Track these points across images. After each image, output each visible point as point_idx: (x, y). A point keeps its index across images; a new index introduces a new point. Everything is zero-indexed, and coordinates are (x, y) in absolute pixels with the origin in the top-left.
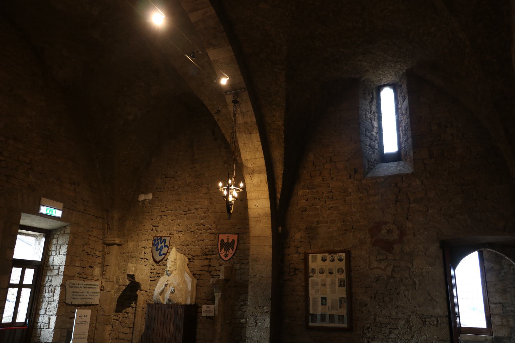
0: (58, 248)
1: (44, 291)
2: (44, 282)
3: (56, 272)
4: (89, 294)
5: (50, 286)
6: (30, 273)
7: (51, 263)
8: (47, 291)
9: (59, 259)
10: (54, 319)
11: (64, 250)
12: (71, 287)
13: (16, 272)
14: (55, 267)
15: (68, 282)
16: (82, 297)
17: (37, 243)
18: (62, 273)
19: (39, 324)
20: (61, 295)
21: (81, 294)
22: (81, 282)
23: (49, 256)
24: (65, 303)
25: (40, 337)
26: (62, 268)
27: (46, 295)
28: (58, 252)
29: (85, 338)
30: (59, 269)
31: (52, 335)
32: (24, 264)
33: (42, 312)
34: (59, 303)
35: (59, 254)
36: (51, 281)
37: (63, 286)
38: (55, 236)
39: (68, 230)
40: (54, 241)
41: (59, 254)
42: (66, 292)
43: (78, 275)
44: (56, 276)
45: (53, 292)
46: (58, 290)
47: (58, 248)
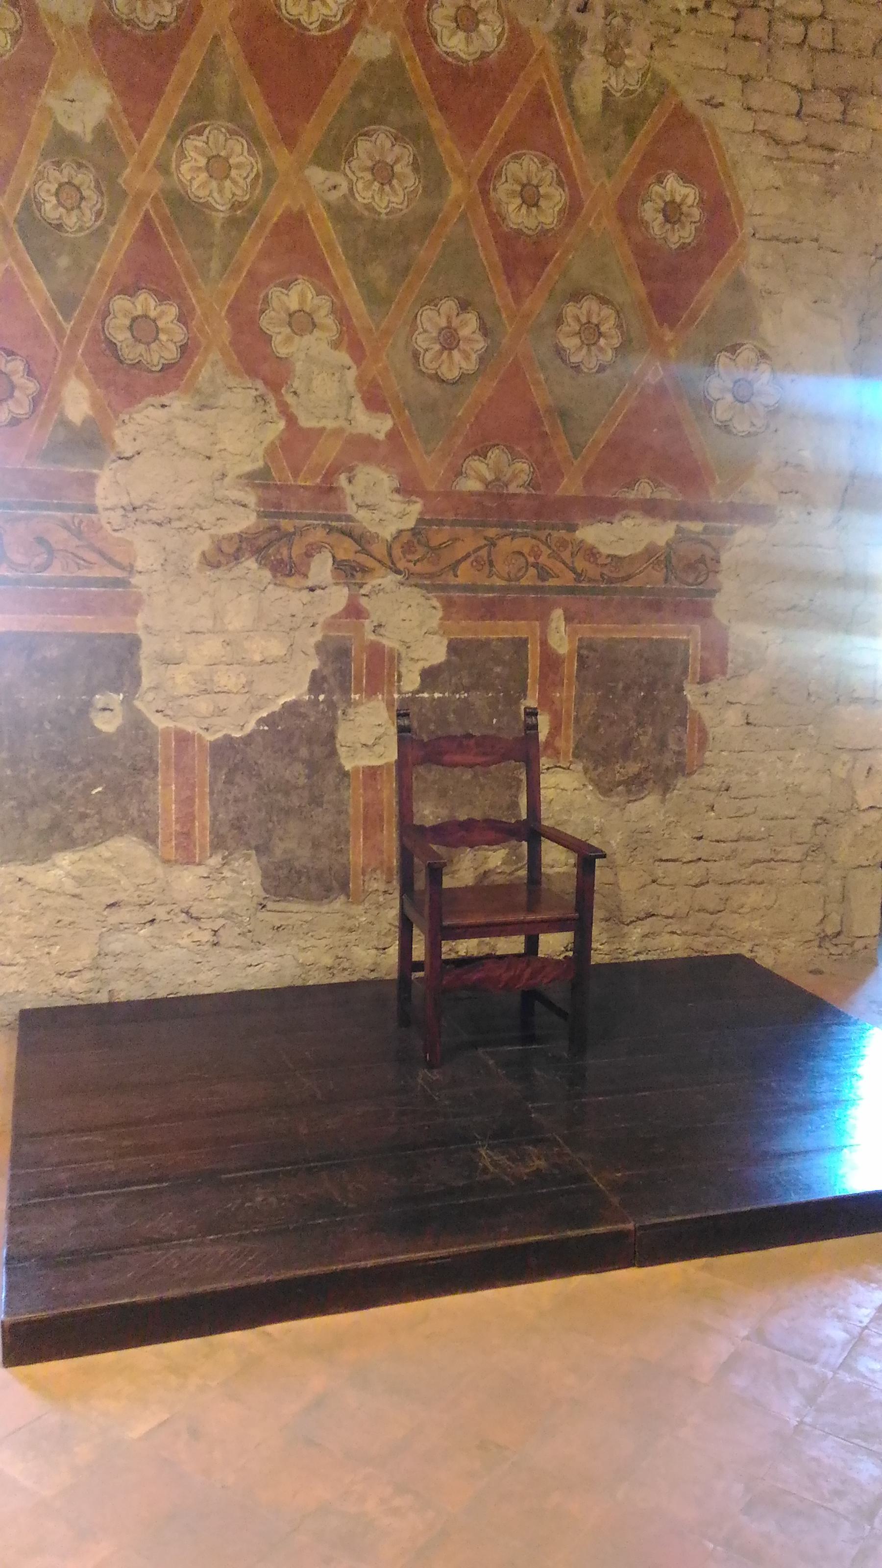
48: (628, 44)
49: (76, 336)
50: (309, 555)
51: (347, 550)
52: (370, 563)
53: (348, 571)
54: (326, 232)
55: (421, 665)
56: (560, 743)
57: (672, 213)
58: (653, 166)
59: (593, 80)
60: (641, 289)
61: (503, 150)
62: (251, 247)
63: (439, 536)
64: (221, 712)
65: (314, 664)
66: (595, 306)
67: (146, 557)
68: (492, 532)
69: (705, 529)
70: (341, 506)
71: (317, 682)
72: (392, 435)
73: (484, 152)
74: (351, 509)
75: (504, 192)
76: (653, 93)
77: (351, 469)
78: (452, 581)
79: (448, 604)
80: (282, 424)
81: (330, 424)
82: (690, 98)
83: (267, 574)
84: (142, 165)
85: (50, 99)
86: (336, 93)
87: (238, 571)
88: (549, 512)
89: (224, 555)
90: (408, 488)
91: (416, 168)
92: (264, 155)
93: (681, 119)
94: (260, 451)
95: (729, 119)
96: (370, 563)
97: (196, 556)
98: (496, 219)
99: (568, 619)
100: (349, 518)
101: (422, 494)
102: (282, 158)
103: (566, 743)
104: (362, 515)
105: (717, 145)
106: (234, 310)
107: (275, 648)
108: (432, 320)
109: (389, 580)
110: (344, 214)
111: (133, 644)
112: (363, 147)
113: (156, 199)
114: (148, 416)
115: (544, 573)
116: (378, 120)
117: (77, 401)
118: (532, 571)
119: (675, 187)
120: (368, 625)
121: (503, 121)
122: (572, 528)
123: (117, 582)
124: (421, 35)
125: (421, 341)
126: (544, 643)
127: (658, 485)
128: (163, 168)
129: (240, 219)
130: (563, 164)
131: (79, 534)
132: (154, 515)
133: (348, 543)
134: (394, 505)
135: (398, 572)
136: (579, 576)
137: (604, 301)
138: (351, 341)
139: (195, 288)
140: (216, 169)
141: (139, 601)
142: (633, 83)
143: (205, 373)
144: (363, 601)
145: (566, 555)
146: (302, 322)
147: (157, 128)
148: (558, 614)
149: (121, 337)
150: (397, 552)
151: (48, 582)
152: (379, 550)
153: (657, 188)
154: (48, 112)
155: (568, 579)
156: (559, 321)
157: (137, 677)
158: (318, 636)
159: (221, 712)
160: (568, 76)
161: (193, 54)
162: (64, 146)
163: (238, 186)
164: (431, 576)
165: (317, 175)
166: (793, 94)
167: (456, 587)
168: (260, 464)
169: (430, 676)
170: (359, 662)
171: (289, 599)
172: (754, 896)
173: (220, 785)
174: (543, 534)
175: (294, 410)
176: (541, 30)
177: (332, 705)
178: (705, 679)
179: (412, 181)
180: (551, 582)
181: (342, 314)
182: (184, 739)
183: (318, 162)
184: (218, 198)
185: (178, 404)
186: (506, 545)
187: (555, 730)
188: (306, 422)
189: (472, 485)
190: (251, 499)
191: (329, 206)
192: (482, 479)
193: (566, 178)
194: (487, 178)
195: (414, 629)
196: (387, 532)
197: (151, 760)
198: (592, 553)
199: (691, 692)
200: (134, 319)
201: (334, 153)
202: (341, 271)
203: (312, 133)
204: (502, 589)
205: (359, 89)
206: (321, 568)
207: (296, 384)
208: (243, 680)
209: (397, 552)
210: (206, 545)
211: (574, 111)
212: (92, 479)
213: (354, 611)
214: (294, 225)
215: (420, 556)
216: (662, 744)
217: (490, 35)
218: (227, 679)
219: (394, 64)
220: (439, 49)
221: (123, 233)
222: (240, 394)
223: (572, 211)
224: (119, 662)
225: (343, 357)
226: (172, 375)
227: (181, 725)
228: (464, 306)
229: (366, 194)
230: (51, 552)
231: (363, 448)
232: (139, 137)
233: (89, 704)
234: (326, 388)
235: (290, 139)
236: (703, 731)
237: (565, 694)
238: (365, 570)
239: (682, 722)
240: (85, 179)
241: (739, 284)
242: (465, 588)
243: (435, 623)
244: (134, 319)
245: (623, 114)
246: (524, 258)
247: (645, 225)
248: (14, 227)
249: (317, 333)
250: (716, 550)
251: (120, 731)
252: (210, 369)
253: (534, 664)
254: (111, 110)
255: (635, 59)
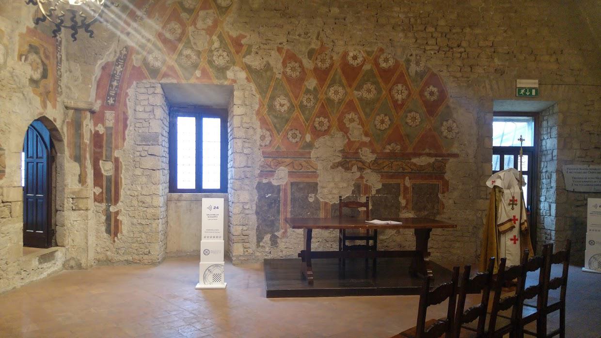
0: (549, 130)
1: (542, 178)
2: (540, 168)
3: (549, 157)
4: (581, 183)
5: (546, 172)
6: (524, 160)
7: (544, 147)
8: (544, 177)
9: (550, 143)
10: (554, 206)
11: (554, 132)
12: (571, 172)
13: (496, 158)
14: (549, 152)
15: (565, 168)
16: (589, 183)
17: (530, 128)
18: (555, 158)
19: (542, 211)
20: (558, 181)
21: (587, 180)
22: (585, 166)
23: (542, 140)
24: (565, 189)
25: (544, 224)
26: (555, 153)
27: (544, 181)
28: (549, 135)
29: (220, 237)
30: (552, 152)
31: (554, 223)
32: (515, 151)
33: (542, 199)
34: (557, 189)
35: (551, 138)
36: (546, 167)
37: (559, 172)
38: (545, 118)
39: (556, 109)
40: (545, 124)
41: (551, 138)
42: (563, 178)
43: (580, 159)
44: (550, 161)
45: (550, 178)
46: (554, 176)
47: (549, 130)
48: (421, 61)
49: (308, 127)
50: (352, 166)
51: (360, 165)
52: (365, 167)
53: (360, 169)
54: (357, 103)
55: (376, 189)
56: (408, 206)
57: (432, 93)
58: (427, 84)
59: (413, 69)
60: (425, 109)
61: (394, 84)
62: (342, 107)
63: (380, 161)
64: (333, 198)
65: (353, 188)
66: (414, 113)
67: (320, 166)
68: (392, 160)
69: (442, 159)
70: (359, 156)
71: (353, 192)
72: (370, 141)
73: (390, 85)
74: (361, 156)
75: (394, 92)
76: (426, 71)
77: (361, 149)
78: (383, 170)
79: (382, 176)
80: (347, 140)
81: (357, 140)
82: (435, 71)
83: (343, 170)
84: (322, 93)
85: (306, 83)
86: (360, 76)
87: (338, 169)
88: (405, 156)
89: (335, 166)
90: (373, 152)
91: (375, 89)
92: (345, 90)
93: (433, 75)
94: (343, 146)
95: (444, 74)
96: (365, 167)
97: (330, 166)
98: (392, 97)
99: (410, 179)
100: (361, 158)
101: (377, 153)
102: (348, 90)
103: (410, 206)
104: (363, 158)
105: (441, 79)
106: (338, 119)
107: (345, 185)
108: (379, 118)
109: (369, 171)
110: (361, 99)
111: (317, 184)
112: (365, 86)
113: (324, 100)
114: (321, 139)
115: (404, 169)
116: (368, 81)
117: (308, 138)
118: (401, 169)
119: (432, 88)
120: (364, 180)
121: (394, 79)
122: (411, 159)
123: (313, 172)
124: (377, 64)
125: (376, 122)
126: (404, 184)
127: (430, 150)
128: (326, 94)
129: (340, 103)
130: (407, 86)
131: (308, 163)
132: (322, 159)
133: (360, 163)
134: (370, 155)
135: (371, 169)
136: (412, 170)
137: (416, 112)
138: (362, 123)
139: (331, 115)
140: (335, 93)
141: (318, 176)
142: (422, 69)
143: (332, 131)
144: (363, 175)
145: (409, 165)
146: (352, 120)
147: (325, 88)
148: (407, 178)
149: (317, 126)
150: (371, 165)
151: (301, 172)
152: (367, 165)
153: (428, 89)
154: (305, 85)
155: (410, 170)
156: (407, 117)
157: (317, 190)
158: (354, 183)
159: (333, 198)
160: (408, 69)
161: (332, 73)
162: (308, 91)
163: (340, 96)
164: (378, 170)
165: (356, 92)
166: (459, 67)
167: (384, 172)
168: (343, 148)
169: (378, 191)
170: (362, 189)
171: (348, 175)
172: (458, 245)
173: (333, 213)
174: (403, 161)
175: (350, 137)
176: (402, 61)
177: (356, 197)
178: (443, 192)
179: (375, 92)
180: (406, 171)
181: (360, 118)
182: (326, 203)
183: (356, 89)
184: (336, 98)
185: (327, 137)
186: (395, 163)
187: (407, 204)
188: (352, 139)
189: (388, 151)
190: (341, 155)
191: (357, 98)
192: (390, 150)
193: (408, 88)
194: (390, 90)
195: (374, 181)
196: (369, 161)
197: (320, 208)
198: (415, 165)
199: (440, 196)
200: (319, 122)
201: (359, 88)
202: (360, 110)
203: (355, 85)
204: (394, 173)
205: (363, 76)
206: (355, 168)
207: (350, 132)
208: (338, 191)
209: (371, 165)
210: (331, 165)
211: (409, 75)
212: (310, 153)
213: (361, 177)
214: (351, 102)
215: (375, 165)
216: (433, 208)
217: (391, 63)
218: (335, 191)
219: (371, 70)
220: (381, 66)
221: (318, 106)
222: (340, 134)
223: (409, 95)
224: (314, 188)
225: (360, 127)
226: (326, 132)
227: (325, 201)
228: (386, 115)
229: (366, 95)
230: (302, 166)
231: (364, 144)
232: (322, 88)
233: (308, 196)
234: (356, 132)
235: (350, 86)
236: (443, 205)
237: (410, 195)
238: (364, 169)
239: (438, 202)
240: (312, 97)
241: (448, 107)
242: (386, 172)
243: (379, 180)
244: (319, 122)
245: (420, 75)
246: (398, 106)
247: (426, 96)
248: (298, 107)
249: (355, 122)
250: (445, 164)
251: (314, 201)
252: (334, 130)
253: (402, 189)
254: (317, 84)
255: (422, 64)
